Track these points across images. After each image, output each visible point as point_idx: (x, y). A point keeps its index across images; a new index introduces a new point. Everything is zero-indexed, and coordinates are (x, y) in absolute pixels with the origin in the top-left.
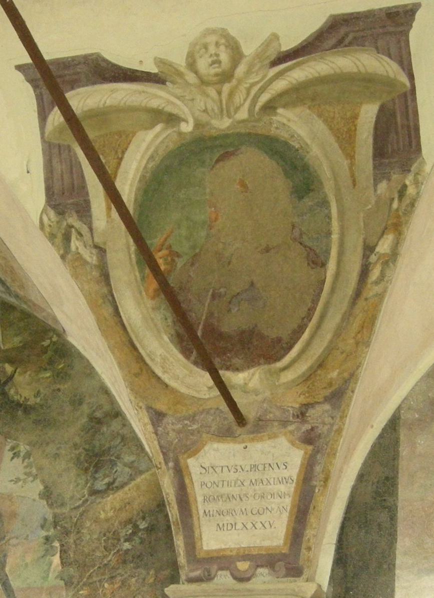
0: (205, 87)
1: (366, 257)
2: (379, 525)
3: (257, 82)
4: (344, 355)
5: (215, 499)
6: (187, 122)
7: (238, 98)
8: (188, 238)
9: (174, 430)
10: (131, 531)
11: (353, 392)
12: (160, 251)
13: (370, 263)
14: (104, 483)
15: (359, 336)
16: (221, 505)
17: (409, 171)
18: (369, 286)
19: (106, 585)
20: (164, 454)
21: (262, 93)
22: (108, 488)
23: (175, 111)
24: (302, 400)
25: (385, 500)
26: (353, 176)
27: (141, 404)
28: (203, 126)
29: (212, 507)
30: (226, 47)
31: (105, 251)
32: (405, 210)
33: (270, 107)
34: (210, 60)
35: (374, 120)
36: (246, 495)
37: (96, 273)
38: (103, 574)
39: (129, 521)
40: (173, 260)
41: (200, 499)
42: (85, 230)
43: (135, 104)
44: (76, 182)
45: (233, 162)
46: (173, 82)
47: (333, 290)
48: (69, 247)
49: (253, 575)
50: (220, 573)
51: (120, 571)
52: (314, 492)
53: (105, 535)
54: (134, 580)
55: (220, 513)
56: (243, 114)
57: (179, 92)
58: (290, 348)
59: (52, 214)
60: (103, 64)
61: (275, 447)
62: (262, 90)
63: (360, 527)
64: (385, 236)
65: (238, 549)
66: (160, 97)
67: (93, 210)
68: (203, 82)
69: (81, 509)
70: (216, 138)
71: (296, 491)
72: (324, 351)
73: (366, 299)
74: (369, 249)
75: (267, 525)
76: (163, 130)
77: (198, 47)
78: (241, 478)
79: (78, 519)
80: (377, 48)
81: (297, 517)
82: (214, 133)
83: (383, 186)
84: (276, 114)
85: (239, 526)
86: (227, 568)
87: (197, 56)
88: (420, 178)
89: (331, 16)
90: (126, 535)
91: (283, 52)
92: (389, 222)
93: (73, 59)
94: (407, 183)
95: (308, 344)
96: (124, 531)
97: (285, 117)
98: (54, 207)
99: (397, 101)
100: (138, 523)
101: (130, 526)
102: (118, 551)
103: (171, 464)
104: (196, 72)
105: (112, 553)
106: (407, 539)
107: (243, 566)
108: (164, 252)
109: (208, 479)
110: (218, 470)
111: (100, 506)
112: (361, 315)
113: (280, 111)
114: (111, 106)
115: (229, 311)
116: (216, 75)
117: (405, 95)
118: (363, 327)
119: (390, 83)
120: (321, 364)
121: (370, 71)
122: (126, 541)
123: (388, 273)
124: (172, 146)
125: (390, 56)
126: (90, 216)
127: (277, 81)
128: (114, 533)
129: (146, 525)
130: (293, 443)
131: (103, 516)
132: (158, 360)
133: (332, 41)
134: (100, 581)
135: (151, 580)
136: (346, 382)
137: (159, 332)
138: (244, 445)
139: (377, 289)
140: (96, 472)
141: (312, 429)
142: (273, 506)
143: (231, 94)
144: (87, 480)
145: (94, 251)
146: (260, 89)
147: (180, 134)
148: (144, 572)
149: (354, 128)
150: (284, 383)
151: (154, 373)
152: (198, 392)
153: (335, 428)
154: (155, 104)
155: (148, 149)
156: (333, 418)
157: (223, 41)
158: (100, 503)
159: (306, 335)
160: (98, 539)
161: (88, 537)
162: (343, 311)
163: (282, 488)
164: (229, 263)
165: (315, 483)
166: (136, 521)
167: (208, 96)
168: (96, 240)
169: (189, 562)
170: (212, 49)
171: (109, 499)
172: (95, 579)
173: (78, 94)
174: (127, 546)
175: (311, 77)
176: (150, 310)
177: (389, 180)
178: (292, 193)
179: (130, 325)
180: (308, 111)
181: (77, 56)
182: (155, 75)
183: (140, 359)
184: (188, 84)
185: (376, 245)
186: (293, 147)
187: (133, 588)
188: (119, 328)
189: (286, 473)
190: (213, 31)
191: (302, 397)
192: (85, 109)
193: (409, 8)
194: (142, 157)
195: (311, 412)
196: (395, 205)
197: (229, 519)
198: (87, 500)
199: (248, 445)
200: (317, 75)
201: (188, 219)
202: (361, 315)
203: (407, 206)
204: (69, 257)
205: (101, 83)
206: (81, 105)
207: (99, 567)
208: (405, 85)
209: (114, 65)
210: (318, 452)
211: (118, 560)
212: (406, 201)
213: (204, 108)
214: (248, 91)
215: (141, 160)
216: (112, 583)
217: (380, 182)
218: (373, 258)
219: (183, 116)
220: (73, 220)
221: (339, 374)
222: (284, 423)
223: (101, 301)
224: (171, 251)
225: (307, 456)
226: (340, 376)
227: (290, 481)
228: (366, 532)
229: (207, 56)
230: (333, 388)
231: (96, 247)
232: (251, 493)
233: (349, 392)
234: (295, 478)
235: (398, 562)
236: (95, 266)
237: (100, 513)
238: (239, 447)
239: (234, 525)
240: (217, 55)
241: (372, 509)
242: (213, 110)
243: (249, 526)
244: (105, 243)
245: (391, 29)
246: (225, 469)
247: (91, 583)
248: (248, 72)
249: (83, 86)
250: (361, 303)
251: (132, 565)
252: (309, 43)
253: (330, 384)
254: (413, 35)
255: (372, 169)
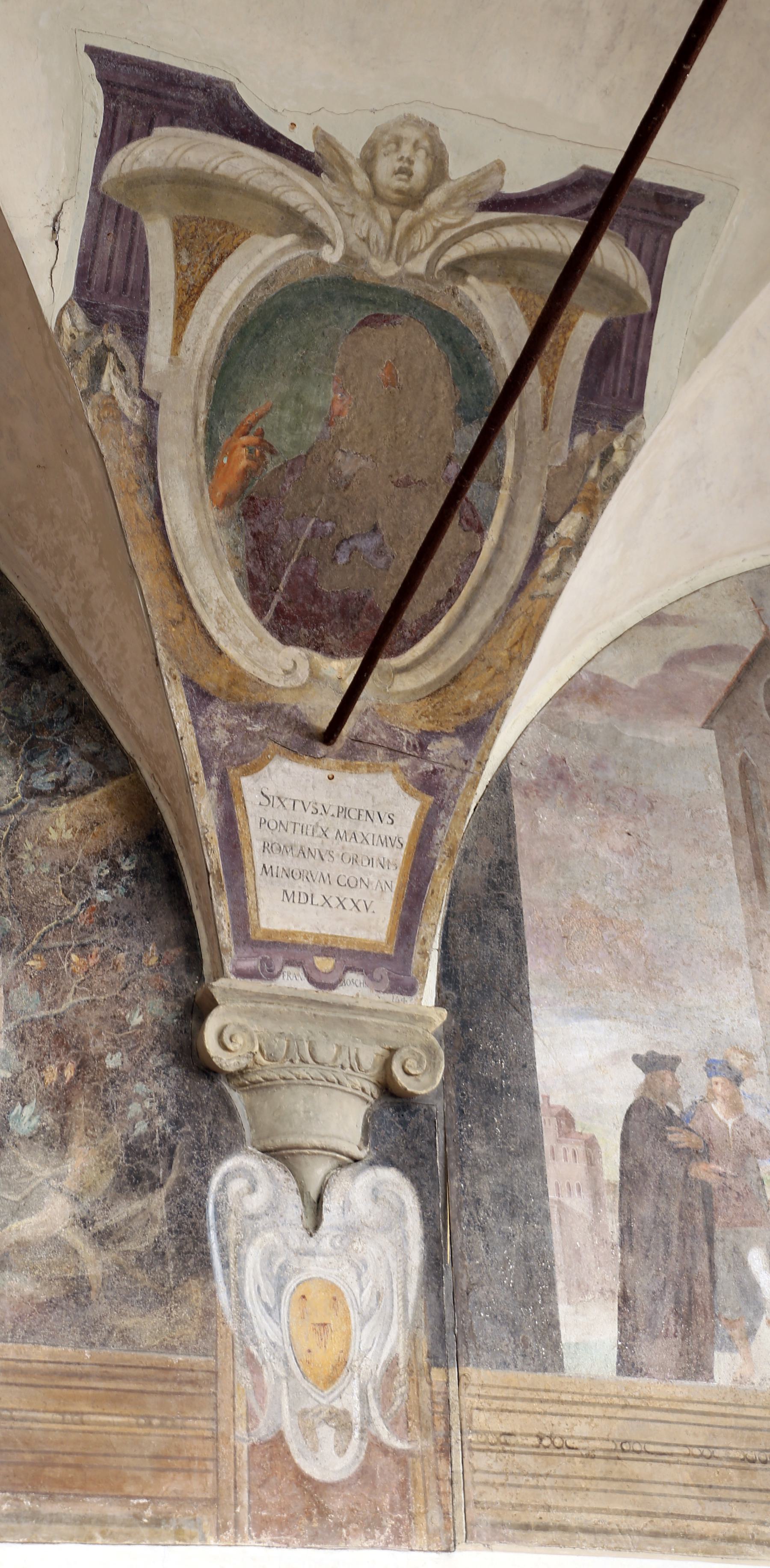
0: (376, 204)
1: (541, 536)
2: (499, 932)
3: (452, 226)
4: (492, 671)
5: (285, 849)
6: (334, 247)
7: (419, 239)
8: (291, 429)
9: (224, 726)
10: (107, 872)
11: (498, 729)
12: (246, 434)
13: (545, 547)
14: (49, 779)
15: (516, 649)
16: (290, 862)
17: (621, 429)
18: (539, 579)
19: (74, 957)
20: (204, 761)
21: (455, 244)
22: (56, 791)
23: (322, 224)
24: (423, 724)
25: (503, 896)
26: (545, 411)
27: (175, 672)
28: (356, 262)
29: (276, 861)
30: (427, 155)
31: (157, 408)
32: (605, 484)
33: (459, 269)
34: (398, 165)
35: (592, 339)
36: (330, 853)
37: (135, 439)
38: (67, 937)
39: (103, 854)
40: (262, 456)
41: (257, 845)
42: (130, 362)
43: (263, 188)
44: (131, 277)
45: (385, 330)
46: (332, 178)
47: (488, 571)
48: (100, 381)
49: (340, 981)
50: (287, 969)
51: (96, 937)
52: (433, 868)
53: (62, 871)
54: (122, 956)
55: (290, 874)
56: (418, 266)
57: (336, 195)
58: (415, 641)
59: (80, 317)
60: (234, 104)
61: (377, 787)
62: (456, 240)
63: (471, 930)
64: (572, 513)
65: (317, 936)
66: (306, 193)
67: (150, 334)
68: (376, 195)
69: (12, 818)
70: (371, 287)
71: (406, 860)
72: (462, 659)
73: (532, 598)
74: (548, 525)
75: (361, 905)
76: (293, 246)
77: (386, 138)
78: (323, 824)
79: (9, 834)
80: (627, 238)
81: (406, 902)
82: (369, 279)
83: (582, 440)
84: (464, 283)
85: (319, 899)
86: (300, 964)
87: (381, 151)
88: (633, 444)
89: (584, 167)
90: (100, 877)
91: (502, 194)
92: (581, 495)
93: (190, 75)
94: (616, 445)
95: (442, 642)
96: (96, 869)
97: (475, 291)
98: (89, 308)
99: (628, 323)
100: (119, 860)
101: (105, 863)
102: (89, 902)
103: (214, 780)
104: (371, 176)
105: (79, 903)
106: (541, 961)
107: (324, 964)
108: (252, 439)
109: (274, 814)
110: (289, 804)
111: (46, 818)
112: (522, 618)
113: (472, 280)
114: (225, 177)
115: (334, 559)
116: (399, 191)
117: (639, 319)
118: (522, 638)
119: (627, 294)
120: (456, 678)
121: (608, 267)
122: (100, 886)
123: (566, 567)
124: (300, 276)
125: (639, 257)
126: (145, 344)
127: (480, 234)
128: (77, 869)
129: (133, 867)
130: (405, 788)
131: (54, 836)
132: (213, 606)
133: (573, 205)
134: (62, 948)
135: (153, 961)
136: (490, 712)
137: (221, 563)
138: (329, 773)
139: (551, 587)
140: (32, 758)
141: (435, 771)
142: (372, 878)
143: (410, 230)
144: (17, 768)
145: (138, 401)
146: (453, 237)
147: (319, 261)
148: (138, 946)
149: (562, 342)
150: (399, 693)
151: (203, 627)
152: (269, 674)
153: (469, 777)
154: (293, 199)
155: (262, 266)
156: (466, 762)
157: (426, 143)
158: (45, 813)
159: (440, 629)
160: (50, 875)
161: (32, 869)
162: (497, 606)
163: (386, 853)
164: (346, 487)
165: (435, 855)
166: (114, 856)
167: (376, 218)
168: (146, 384)
169: (236, 942)
170: (406, 150)
171: (61, 808)
172: (52, 943)
173: (176, 136)
174: (103, 895)
175: (528, 245)
176: (212, 524)
177: (593, 434)
178: (458, 408)
179: (176, 538)
180: (508, 294)
181: (197, 75)
182: (309, 155)
183: (184, 598)
184: (352, 188)
185: (559, 522)
186: (476, 341)
187: (122, 969)
188: (157, 539)
189: (392, 831)
190: (418, 123)
191: (424, 719)
192: (182, 165)
193: (687, 197)
194: (250, 276)
195: (438, 749)
196: (593, 472)
197: (301, 886)
198: (21, 804)
199: (336, 774)
200: (536, 246)
201: (298, 398)
202: (522, 618)
203: (609, 478)
204: (96, 398)
205: (220, 133)
206: (176, 155)
207: (59, 925)
208: (645, 304)
209: (250, 113)
210: (441, 808)
211: (90, 918)
212: (608, 472)
213: (364, 235)
214: (437, 233)
215: (246, 281)
216: (85, 955)
217: (580, 432)
218: (550, 541)
219: (330, 236)
220: (112, 337)
221: (481, 697)
222: (394, 752)
223: (133, 487)
224: (262, 440)
225: (425, 812)
226: (483, 702)
227: (397, 843)
228: (482, 939)
229: (395, 157)
230: (471, 717)
231: (143, 395)
232: (337, 851)
233: (492, 728)
234: (405, 840)
235: (533, 994)
236: (137, 427)
237: (48, 830)
238: (323, 775)
239: (309, 898)
240: (411, 162)
241: (486, 906)
242: (377, 242)
243: (334, 902)
244: (159, 395)
245: (653, 218)
246: (298, 805)
247: (48, 950)
248: (446, 206)
249: (189, 126)
250: (524, 601)
251: (116, 929)
252: (542, 196)
253: (467, 711)
254: (679, 236)
255: (573, 409)
